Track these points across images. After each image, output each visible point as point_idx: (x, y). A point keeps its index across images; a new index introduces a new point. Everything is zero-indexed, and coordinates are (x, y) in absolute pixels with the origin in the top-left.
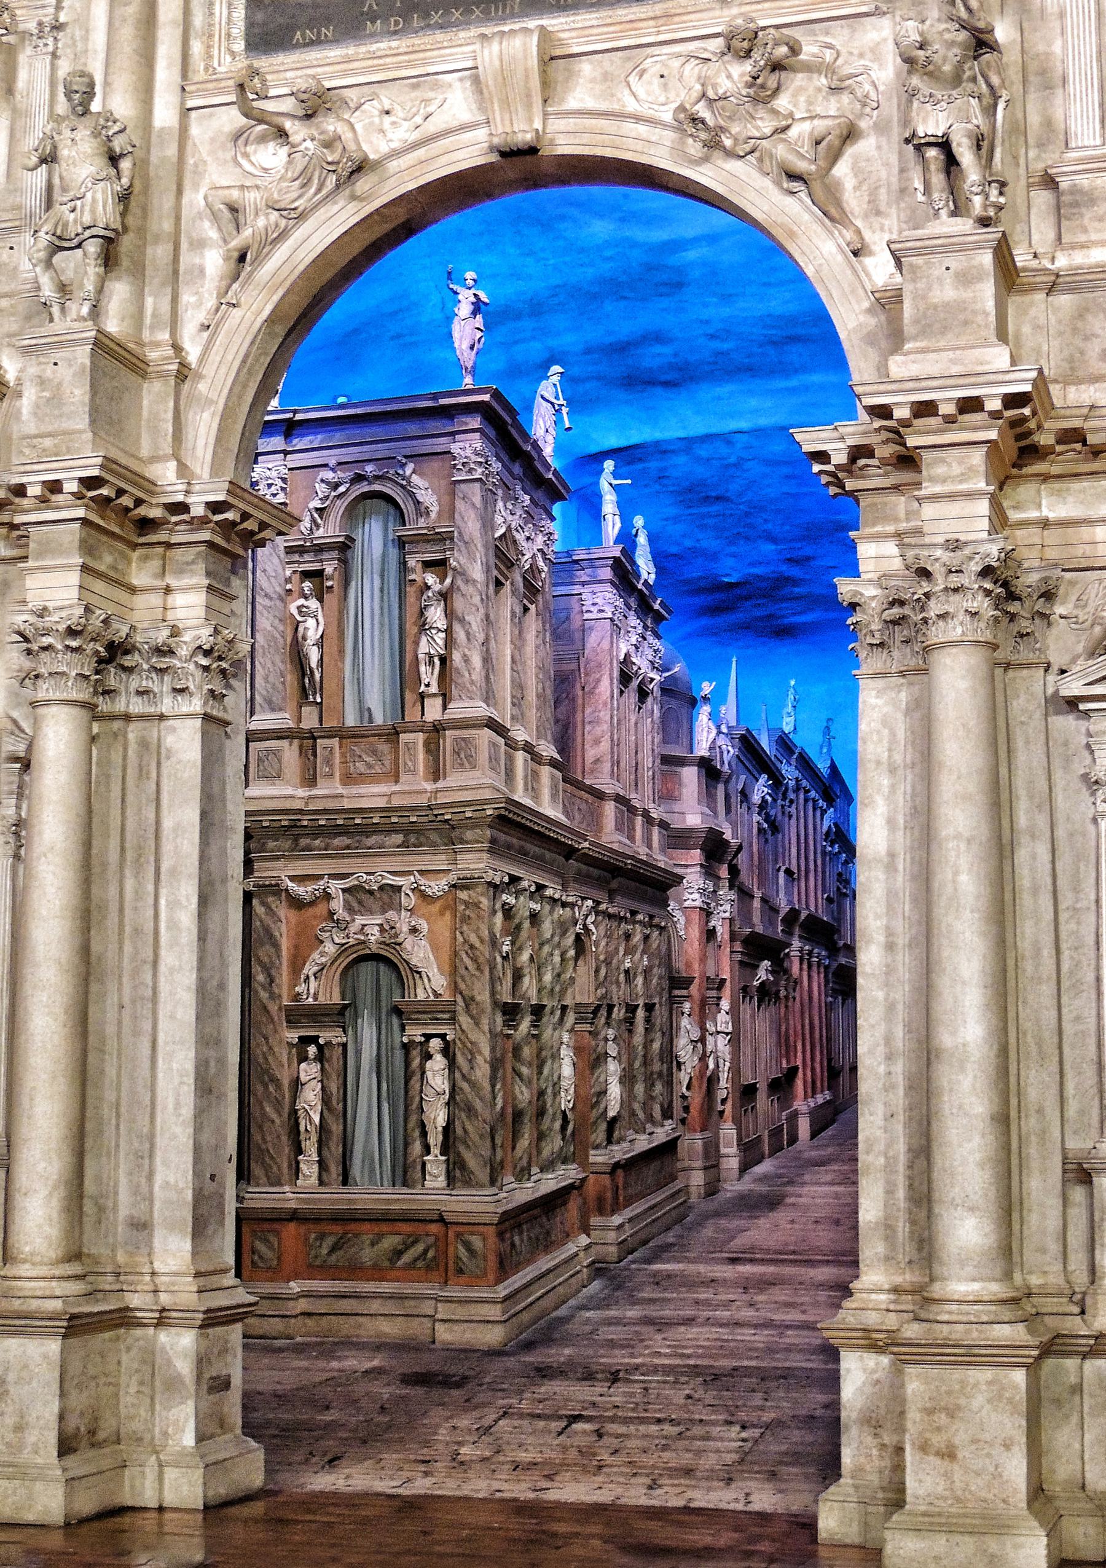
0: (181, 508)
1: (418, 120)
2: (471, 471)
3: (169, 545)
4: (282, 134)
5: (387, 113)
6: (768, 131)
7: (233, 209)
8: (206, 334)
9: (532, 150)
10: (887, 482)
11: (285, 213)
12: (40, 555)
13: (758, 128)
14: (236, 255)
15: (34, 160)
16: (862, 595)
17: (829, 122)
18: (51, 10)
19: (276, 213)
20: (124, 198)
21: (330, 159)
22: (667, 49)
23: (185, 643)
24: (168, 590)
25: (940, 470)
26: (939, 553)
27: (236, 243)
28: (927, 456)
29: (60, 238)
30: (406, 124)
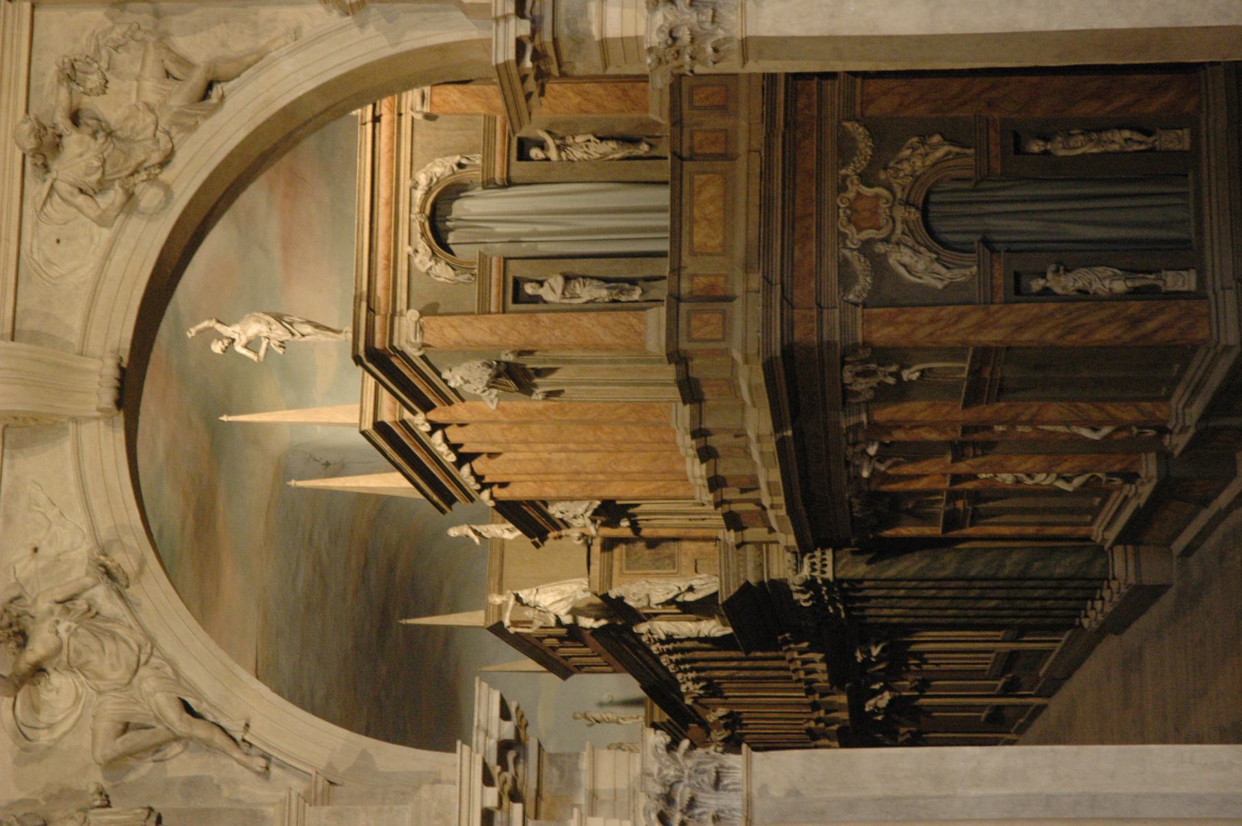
1: (52, 513)
4: (38, 670)
5: (36, 550)
6: (150, 119)
7: (126, 728)
8: (274, 770)
9: (122, 371)
11: (143, 659)
13: (144, 129)
14: (186, 716)
16: (662, 26)
17: (151, 58)
19: (143, 671)
20: (108, 805)
21: (85, 607)
23: (660, 770)
24: (593, 795)
27: (173, 715)
30: (54, 528)
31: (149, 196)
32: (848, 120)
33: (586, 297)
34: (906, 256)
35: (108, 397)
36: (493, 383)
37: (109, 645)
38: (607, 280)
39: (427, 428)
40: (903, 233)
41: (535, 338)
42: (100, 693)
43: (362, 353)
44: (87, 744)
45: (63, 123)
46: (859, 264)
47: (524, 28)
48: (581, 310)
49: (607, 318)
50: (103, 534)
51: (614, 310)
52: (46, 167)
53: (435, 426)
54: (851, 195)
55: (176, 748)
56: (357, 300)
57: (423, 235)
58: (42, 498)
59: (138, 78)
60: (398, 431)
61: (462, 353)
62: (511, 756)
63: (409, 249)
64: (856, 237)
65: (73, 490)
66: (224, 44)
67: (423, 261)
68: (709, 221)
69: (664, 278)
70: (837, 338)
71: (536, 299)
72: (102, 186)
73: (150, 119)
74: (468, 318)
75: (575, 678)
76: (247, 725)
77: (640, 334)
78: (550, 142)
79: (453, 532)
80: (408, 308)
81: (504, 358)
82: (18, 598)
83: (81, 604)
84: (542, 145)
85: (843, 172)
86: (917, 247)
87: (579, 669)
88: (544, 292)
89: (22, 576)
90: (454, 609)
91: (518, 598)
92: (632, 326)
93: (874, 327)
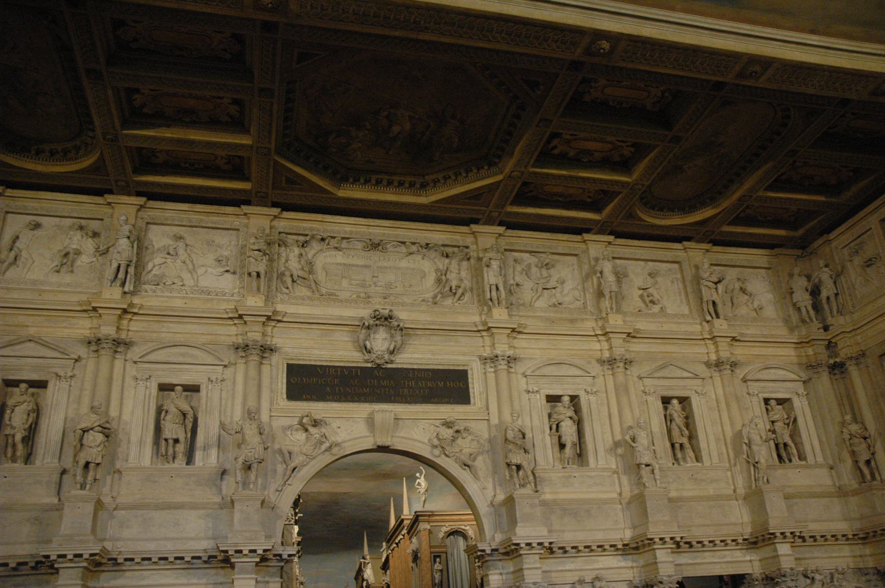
0: (280, 555)
1: (349, 431)
2: (290, 521)
3: (268, 566)
4: (306, 430)
6: (458, 451)
7: (290, 453)
8: (278, 493)
9: (388, 447)
10: (498, 558)
12: (239, 573)
14: (292, 469)
15: (234, 432)
17: (474, 450)
18: (220, 374)
19: (305, 457)
20: (265, 449)
22: (424, 421)
24: (268, 582)
25: (528, 560)
26: (530, 585)
27: (293, 465)
28: (524, 556)
29: (246, 461)
31: (437, 452)
33: (436, 576)
35: (380, 444)
36: (413, 551)
37: (312, 448)
38: (441, 582)
39: (403, 533)
42: (300, 446)
44: (287, 443)
45: (456, 428)
47: (488, 552)
48: (433, 576)
49: (430, 583)
50: (343, 445)
51: (433, 584)
52: (443, 425)
53: (404, 536)
55: (285, 466)
56: (432, 512)
57: (452, 529)
58: (353, 429)
59: (469, 447)
60: (402, 526)
61: (420, 543)
62: (278, 558)
63: (447, 525)
65: (356, 436)
66: (481, 469)
67: (444, 529)
71: (435, 562)
72: (439, 439)
73: (458, 451)
74: (428, 543)
75: (355, 582)
76: (290, 485)
78: (480, 564)
79: (384, 544)
80: (431, 526)
81: (419, 554)
82: (326, 424)
83: (324, 440)
84: (479, 562)
87: (357, 583)
88: (437, 564)
89: (332, 425)
90: (369, 546)
91: (368, 563)
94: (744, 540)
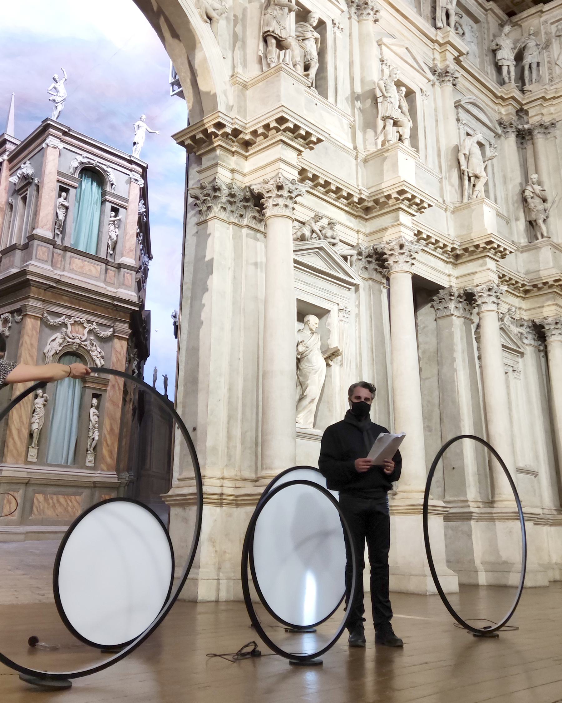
32: (114, 332)
34: (59, 340)
40: (68, 342)
41: (45, 187)
43: (49, 122)
46: (58, 320)
54: (85, 325)
57: (89, 163)
64: (70, 322)
68: (83, 266)
69: (62, 244)
70: (29, 304)
77: (42, 228)
85: (94, 323)
86: (63, 346)
92: (46, 225)
93: (32, 320)
94: (453, 249)
